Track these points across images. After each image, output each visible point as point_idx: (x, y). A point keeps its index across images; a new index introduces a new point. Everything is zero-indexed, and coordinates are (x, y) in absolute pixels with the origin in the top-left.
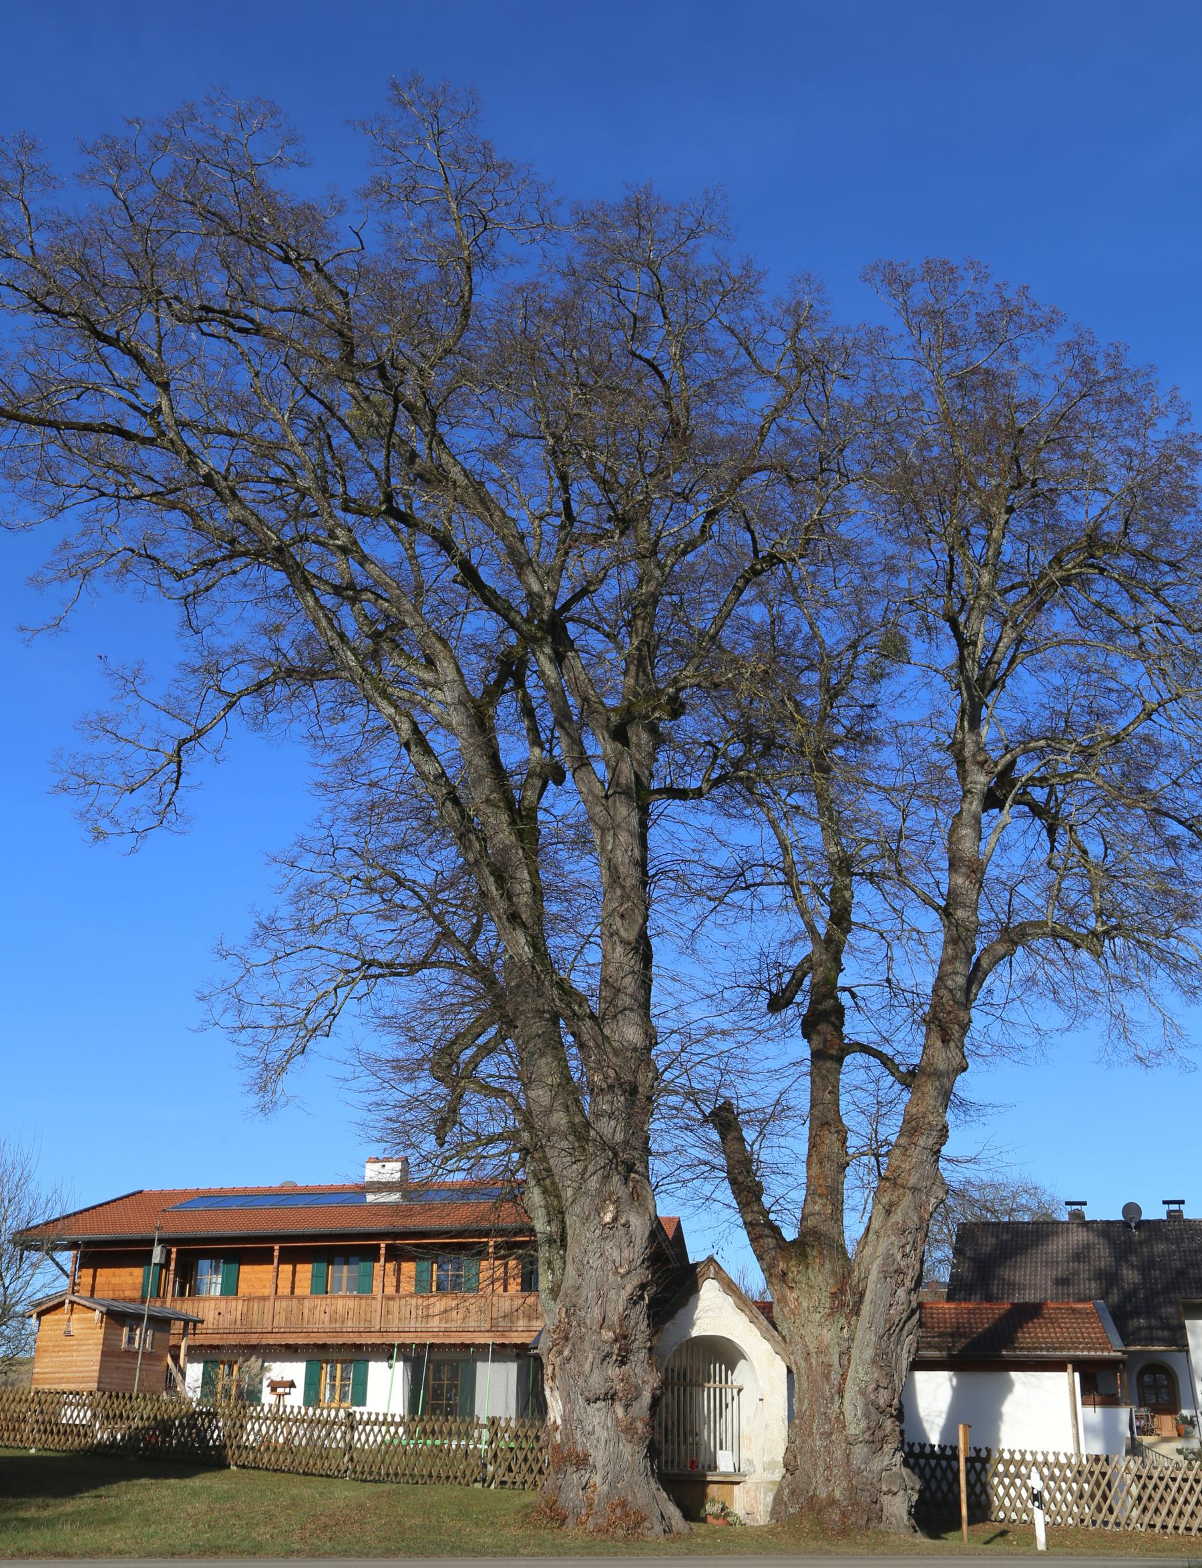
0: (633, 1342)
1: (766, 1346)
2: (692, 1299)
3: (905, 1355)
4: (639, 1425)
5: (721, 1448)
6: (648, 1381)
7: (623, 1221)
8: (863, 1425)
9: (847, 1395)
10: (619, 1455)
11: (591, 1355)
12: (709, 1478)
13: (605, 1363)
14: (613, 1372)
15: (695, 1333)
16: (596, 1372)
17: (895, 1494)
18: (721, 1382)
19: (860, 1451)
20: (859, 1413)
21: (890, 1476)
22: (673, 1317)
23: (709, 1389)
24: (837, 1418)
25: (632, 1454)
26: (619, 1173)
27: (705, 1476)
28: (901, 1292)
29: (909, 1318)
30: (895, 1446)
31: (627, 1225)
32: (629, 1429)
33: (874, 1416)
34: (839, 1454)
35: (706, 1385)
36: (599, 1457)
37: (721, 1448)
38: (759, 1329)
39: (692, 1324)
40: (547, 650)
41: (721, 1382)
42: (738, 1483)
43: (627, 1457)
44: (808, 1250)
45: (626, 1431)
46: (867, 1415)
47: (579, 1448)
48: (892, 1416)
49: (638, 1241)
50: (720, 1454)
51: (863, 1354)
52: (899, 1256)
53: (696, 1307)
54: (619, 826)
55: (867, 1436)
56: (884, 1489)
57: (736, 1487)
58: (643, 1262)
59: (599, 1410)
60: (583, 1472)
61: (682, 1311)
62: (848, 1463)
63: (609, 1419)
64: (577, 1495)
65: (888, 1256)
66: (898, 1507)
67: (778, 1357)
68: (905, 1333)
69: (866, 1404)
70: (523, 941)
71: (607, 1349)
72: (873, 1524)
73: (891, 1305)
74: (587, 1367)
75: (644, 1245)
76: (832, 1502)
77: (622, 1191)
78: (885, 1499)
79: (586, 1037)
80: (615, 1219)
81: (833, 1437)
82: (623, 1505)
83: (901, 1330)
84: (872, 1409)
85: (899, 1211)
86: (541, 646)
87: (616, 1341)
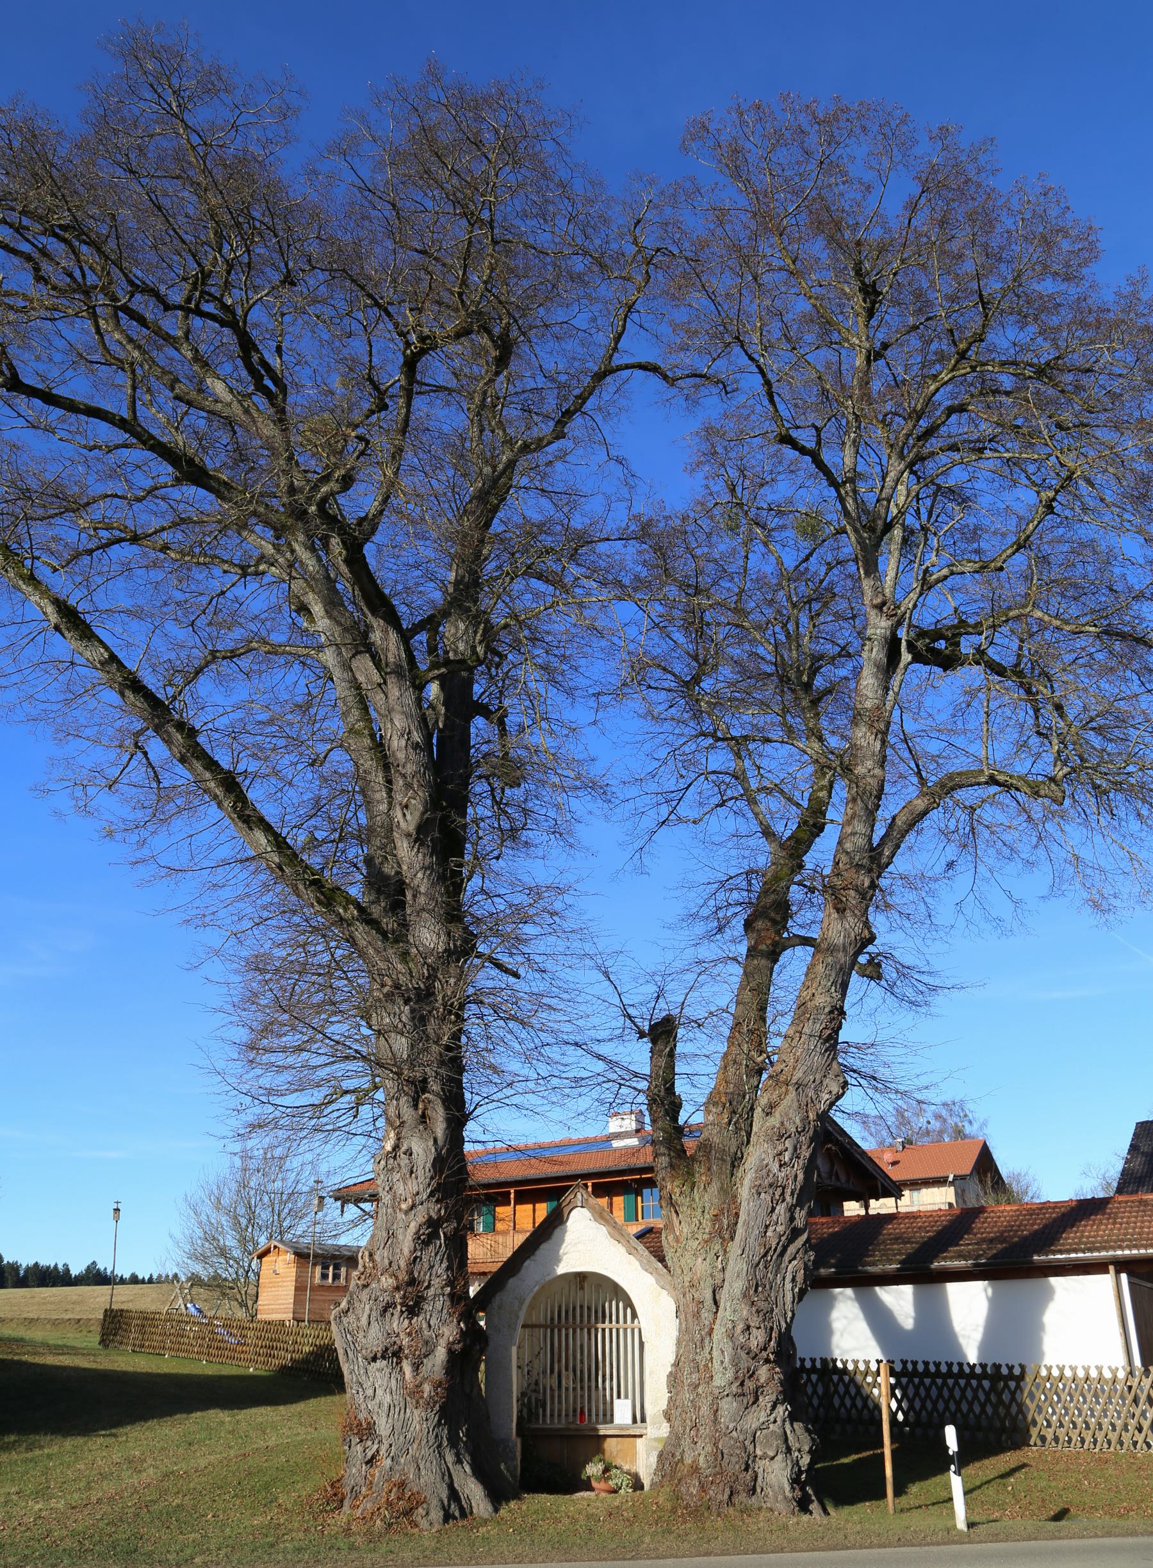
0: (428, 1287)
1: (649, 1280)
2: (557, 1232)
3: (788, 1286)
4: (427, 1388)
5: (619, 1397)
6: (447, 1332)
7: (403, 1149)
8: (730, 1374)
9: (715, 1337)
10: (405, 1425)
11: (367, 1307)
12: (602, 1433)
13: (388, 1315)
14: (398, 1323)
15: (561, 1270)
16: (374, 1324)
17: (772, 1458)
18: (618, 1322)
19: (728, 1406)
20: (727, 1360)
21: (766, 1437)
22: (533, 1254)
23: (603, 1330)
24: (706, 1366)
25: (420, 1421)
26: (406, 1094)
27: (597, 1430)
28: (781, 1209)
29: (791, 1241)
30: (774, 1398)
31: (409, 1153)
32: (416, 1391)
33: (745, 1362)
34: (705, 1410)
35: (600, 1326)
36: (383, 1427)
37: (619, 1397)
38: (641, 1262)
39: (557, 1260)
40: (301, 537)
41: (618, 1322)
42: (641, 1436)
43: (416, 1426)
44: (696, 1166)
45: (412, 1394)
46: (735, 1363)
47: (361, 1416)
48: (767, 1361)
49: (420, 1172)
50: (616, 1402)
51: (734, 1287)
52: (775, 1167)
53: (563, 1241)
54: (393, 709)
55: (734, 1388)
56: (759, 1452)
57: (639, 1440)
58: (432, 1194)
59: (381, 1370)
60: (369, 1443)
61: (544, 1246)
62: (715, 1421)
63: (393, 1381)
64: (360, 1471)
65: (763, 1167)
66: (776, 1474)
67: (665, 1292)
68: (786, 1258)
69: (735, 1349)
70: (264, 841)
71: (386, 1298)
72: (742, 1498)
73: (767, 1227)
74: (364, 1321)
75: (429, 1175)
76: (695, 1469)
77: (408, 1114)
78: (760, 1465)
79: (362, 943)
80: (396, 1147)
81: (700, 1390)
82: (402, 1485)
83: (782, 1254)
84: (743, 1355)
85: (777, 1114)
86: (294, 534)
87: (397, 1289)
